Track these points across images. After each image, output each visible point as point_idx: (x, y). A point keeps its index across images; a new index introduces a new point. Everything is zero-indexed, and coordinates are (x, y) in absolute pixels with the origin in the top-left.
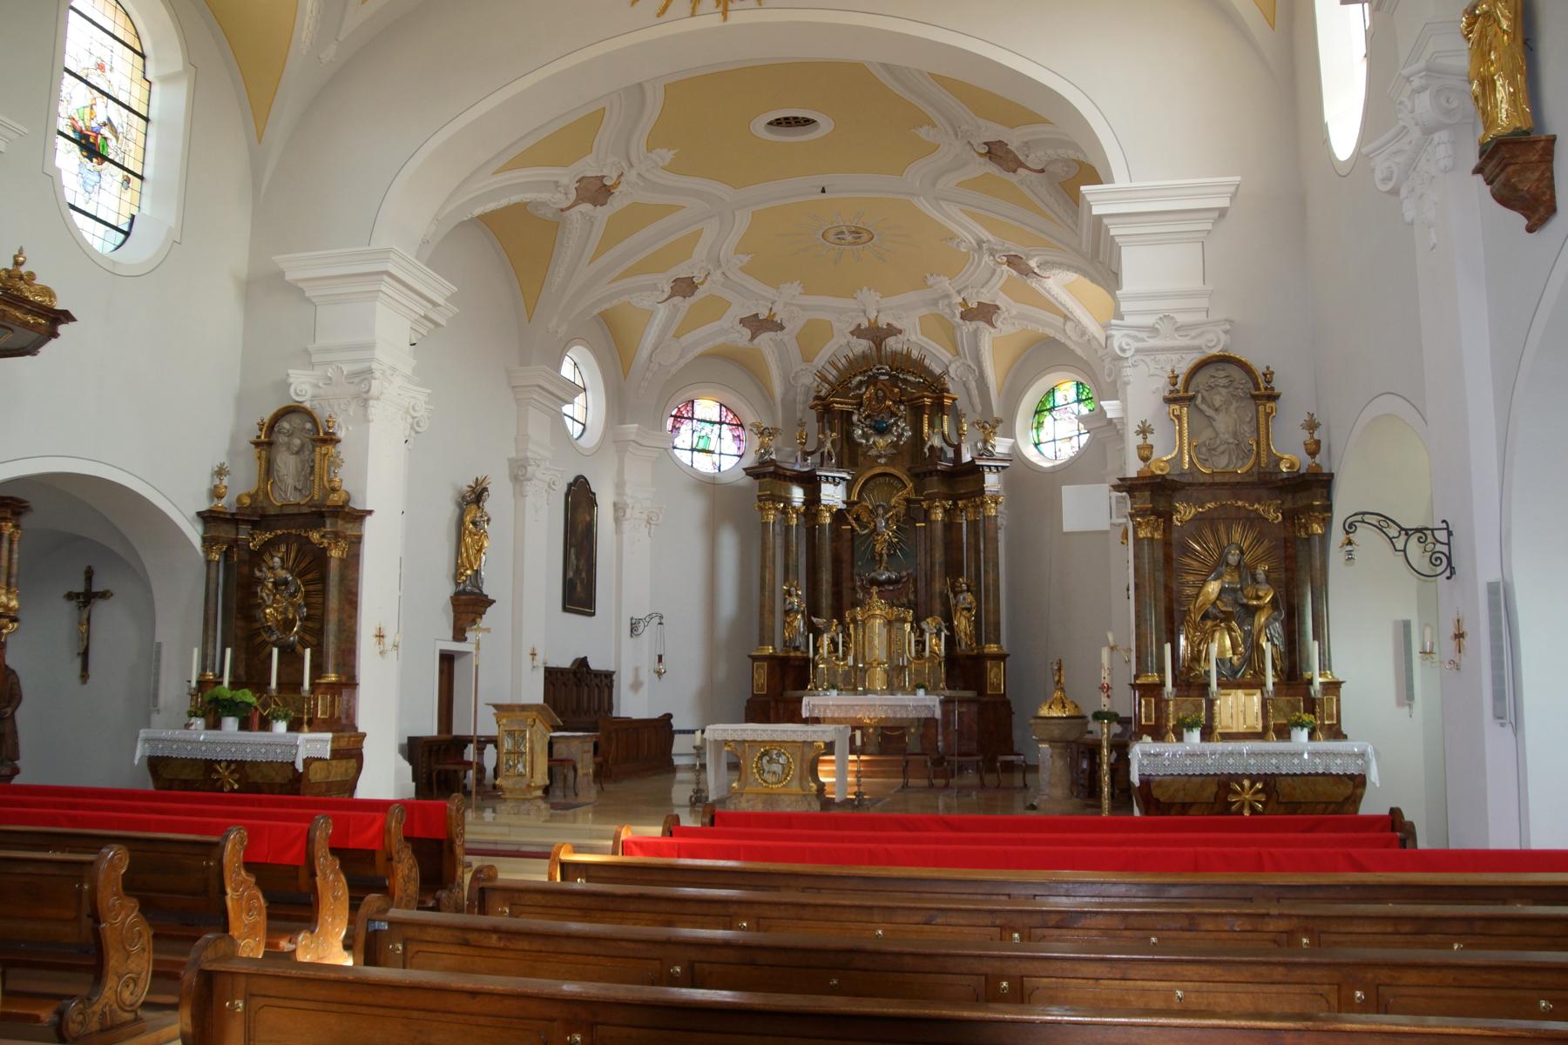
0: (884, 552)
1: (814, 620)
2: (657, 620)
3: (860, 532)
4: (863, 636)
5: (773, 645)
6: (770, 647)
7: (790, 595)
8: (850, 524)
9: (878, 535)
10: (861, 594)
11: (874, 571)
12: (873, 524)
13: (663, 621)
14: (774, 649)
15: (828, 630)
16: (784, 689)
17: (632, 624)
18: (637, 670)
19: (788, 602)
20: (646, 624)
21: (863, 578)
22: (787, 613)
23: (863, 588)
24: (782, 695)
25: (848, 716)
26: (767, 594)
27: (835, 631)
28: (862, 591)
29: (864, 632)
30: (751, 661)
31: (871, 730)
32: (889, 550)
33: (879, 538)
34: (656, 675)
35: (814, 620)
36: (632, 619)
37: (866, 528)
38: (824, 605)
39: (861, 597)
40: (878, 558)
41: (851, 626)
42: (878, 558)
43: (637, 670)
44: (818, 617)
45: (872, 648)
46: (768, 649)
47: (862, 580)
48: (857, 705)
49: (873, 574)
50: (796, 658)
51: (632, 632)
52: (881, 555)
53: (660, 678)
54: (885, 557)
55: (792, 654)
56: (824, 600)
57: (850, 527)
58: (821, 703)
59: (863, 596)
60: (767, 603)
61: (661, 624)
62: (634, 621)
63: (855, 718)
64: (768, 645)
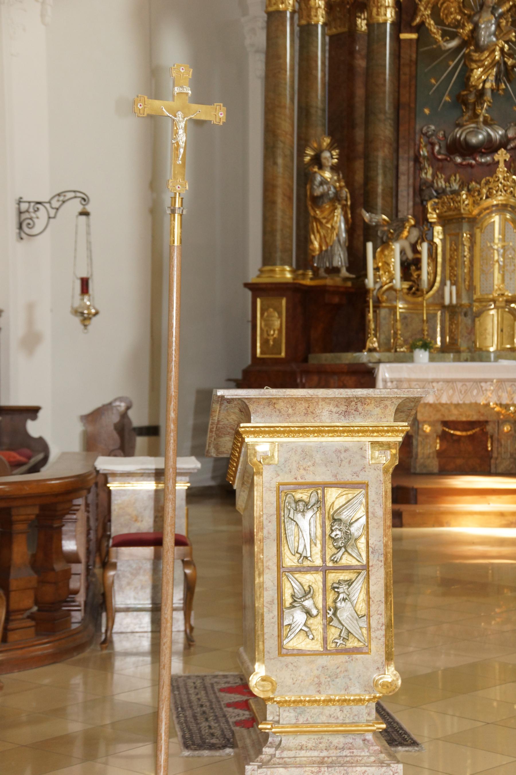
0: (488, 85)
1: (367, 216)
2: (76, 206)
3: (442, 43)
4: (471, 249)
5: (291, 265)
6: (288, 268)
7: (321, 167)
8: (421, 28)
9: (479, 49)
10: (430, 171)
11: (459, 126)
12: (469, 27)
13: (89, 208)
14: (293, 272)
15: (397, 238)
16: (309, 350)
17: (20, 213)
18: (30, 308)
19: (319, 178)
20: (52, 213)
21: (434, 139)
22: (317, 201)
23: (432, 158)
24: (306, 360)
25: (467, 402)
26: (280, 161)
27: (407, 238)
28: (431, 165)
29: (472, 237)
30: (249, 294)
31: (506, 428)
32: (498, 80)
33: (486, 54)
34: (77, 320)
35: (367, 216)
36: (20, 201)
37: (453, 36)
38: (380, 189)
39: (429, 177)
40: (472, 99)
41: (438, 229)
42: (472, 99)
43: (30, 308)
44: (372, 213)
45: (488, 274)
46: (283, 271)
47: (433, 145)
48: (486, 381)
49: (459, 133)
50: (336, 291)
51: (20, 227)
52: (481, 93)
53: (85, 326)
54: (488, 96)
55: (329, 282)
56: (380, 179)
57: (414, 36)
58: (413, 376)
59: (434, 175)
60: (280, 182)
61: (85, 213)
62: (24, 206)
63: (477, 404)
64: (283, 263)
